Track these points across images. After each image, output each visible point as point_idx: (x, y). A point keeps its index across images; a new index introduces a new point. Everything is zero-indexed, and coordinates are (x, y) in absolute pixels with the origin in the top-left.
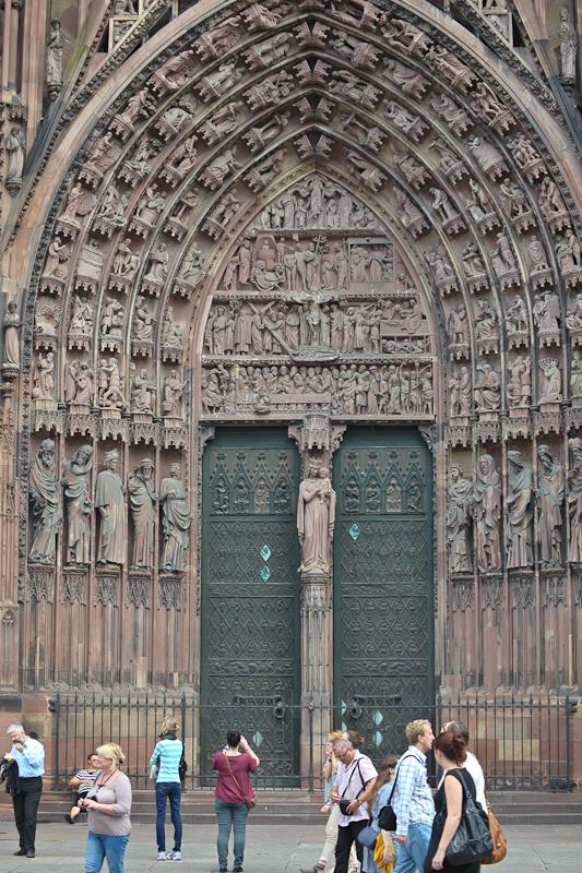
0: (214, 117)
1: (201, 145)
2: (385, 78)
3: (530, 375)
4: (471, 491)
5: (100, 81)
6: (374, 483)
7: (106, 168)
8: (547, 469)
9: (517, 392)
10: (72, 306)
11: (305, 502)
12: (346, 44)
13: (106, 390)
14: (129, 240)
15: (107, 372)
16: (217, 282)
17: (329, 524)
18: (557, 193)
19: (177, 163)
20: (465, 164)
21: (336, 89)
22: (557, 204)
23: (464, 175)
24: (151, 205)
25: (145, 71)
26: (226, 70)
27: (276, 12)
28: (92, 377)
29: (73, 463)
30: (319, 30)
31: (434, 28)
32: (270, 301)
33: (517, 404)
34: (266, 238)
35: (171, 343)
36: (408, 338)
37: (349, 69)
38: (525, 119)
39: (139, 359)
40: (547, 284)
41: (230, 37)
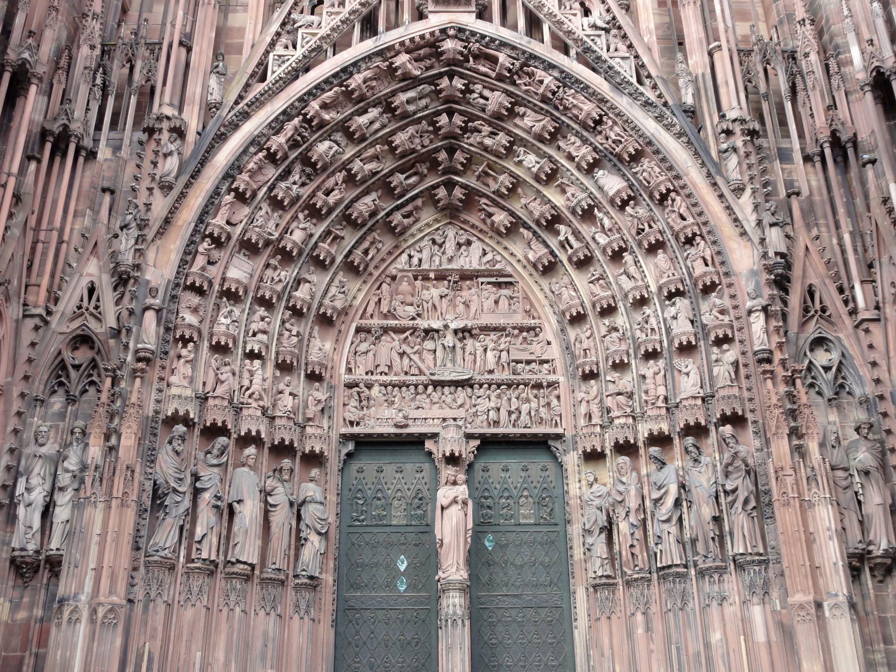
0: (363, 156)
1: (350, 179)
2: (516, 125)
3: (665, 376)
4: (609, 494)
5: (258, 103)
6: (506, 494)
7: (261, 184)
8: (696, 460)
9: (652, 392)
10: (218, 307)
11: (443, 508)
12: (482, 97)
13: (248, 389)
14: (279, 257)
15: (250, 371)
16: (361, 312)
17: (466, 531)
18: (684, 204)
19: (328, 193)
20: (591, 195)
21: (471, 140)
22: (685, 214)
23: (589, 205)
24: (301, 226)
25: (301, 99)
26: (374, 113)
27: (422, 65)
28: (234, 374)
29: (208, 452)
30: (459, 83)
31: (562, 72)
32: (408, 329)
33: (653, 404)
34: (405, 276)
35: (314, 356)
36: (535, 361)
37: (484, 120)
38: (650, 143)
39: (284, 367)
40: (678, 290)
41: (380, 82)
